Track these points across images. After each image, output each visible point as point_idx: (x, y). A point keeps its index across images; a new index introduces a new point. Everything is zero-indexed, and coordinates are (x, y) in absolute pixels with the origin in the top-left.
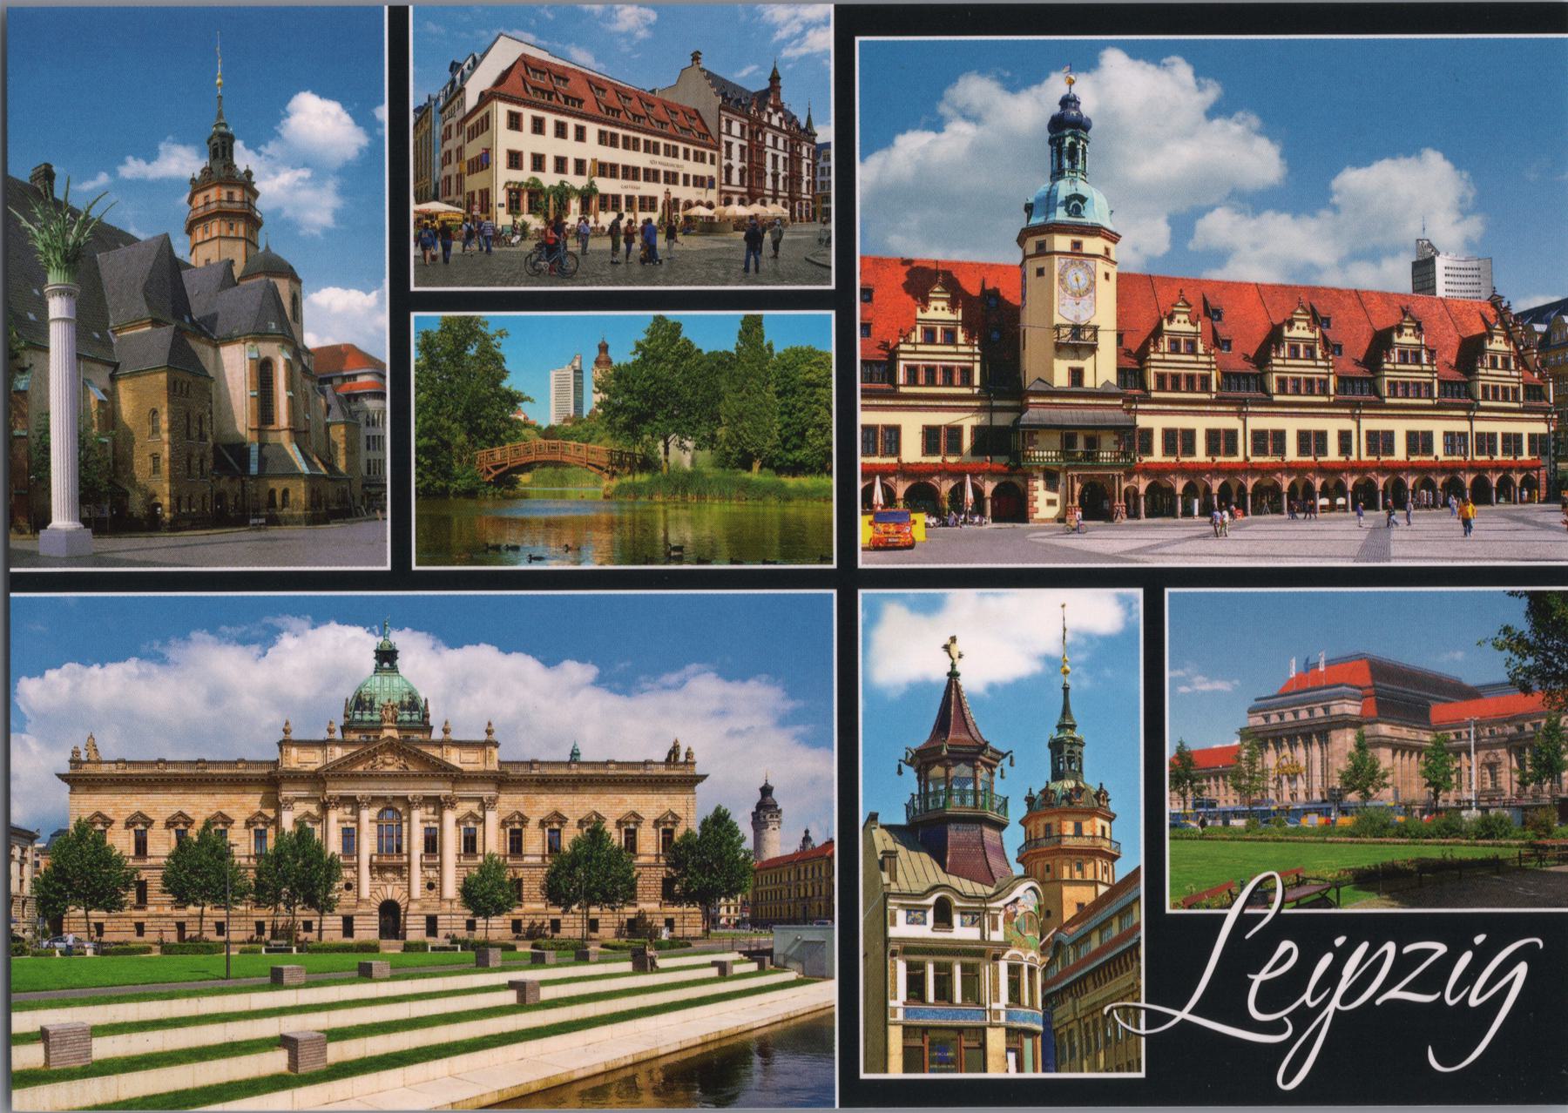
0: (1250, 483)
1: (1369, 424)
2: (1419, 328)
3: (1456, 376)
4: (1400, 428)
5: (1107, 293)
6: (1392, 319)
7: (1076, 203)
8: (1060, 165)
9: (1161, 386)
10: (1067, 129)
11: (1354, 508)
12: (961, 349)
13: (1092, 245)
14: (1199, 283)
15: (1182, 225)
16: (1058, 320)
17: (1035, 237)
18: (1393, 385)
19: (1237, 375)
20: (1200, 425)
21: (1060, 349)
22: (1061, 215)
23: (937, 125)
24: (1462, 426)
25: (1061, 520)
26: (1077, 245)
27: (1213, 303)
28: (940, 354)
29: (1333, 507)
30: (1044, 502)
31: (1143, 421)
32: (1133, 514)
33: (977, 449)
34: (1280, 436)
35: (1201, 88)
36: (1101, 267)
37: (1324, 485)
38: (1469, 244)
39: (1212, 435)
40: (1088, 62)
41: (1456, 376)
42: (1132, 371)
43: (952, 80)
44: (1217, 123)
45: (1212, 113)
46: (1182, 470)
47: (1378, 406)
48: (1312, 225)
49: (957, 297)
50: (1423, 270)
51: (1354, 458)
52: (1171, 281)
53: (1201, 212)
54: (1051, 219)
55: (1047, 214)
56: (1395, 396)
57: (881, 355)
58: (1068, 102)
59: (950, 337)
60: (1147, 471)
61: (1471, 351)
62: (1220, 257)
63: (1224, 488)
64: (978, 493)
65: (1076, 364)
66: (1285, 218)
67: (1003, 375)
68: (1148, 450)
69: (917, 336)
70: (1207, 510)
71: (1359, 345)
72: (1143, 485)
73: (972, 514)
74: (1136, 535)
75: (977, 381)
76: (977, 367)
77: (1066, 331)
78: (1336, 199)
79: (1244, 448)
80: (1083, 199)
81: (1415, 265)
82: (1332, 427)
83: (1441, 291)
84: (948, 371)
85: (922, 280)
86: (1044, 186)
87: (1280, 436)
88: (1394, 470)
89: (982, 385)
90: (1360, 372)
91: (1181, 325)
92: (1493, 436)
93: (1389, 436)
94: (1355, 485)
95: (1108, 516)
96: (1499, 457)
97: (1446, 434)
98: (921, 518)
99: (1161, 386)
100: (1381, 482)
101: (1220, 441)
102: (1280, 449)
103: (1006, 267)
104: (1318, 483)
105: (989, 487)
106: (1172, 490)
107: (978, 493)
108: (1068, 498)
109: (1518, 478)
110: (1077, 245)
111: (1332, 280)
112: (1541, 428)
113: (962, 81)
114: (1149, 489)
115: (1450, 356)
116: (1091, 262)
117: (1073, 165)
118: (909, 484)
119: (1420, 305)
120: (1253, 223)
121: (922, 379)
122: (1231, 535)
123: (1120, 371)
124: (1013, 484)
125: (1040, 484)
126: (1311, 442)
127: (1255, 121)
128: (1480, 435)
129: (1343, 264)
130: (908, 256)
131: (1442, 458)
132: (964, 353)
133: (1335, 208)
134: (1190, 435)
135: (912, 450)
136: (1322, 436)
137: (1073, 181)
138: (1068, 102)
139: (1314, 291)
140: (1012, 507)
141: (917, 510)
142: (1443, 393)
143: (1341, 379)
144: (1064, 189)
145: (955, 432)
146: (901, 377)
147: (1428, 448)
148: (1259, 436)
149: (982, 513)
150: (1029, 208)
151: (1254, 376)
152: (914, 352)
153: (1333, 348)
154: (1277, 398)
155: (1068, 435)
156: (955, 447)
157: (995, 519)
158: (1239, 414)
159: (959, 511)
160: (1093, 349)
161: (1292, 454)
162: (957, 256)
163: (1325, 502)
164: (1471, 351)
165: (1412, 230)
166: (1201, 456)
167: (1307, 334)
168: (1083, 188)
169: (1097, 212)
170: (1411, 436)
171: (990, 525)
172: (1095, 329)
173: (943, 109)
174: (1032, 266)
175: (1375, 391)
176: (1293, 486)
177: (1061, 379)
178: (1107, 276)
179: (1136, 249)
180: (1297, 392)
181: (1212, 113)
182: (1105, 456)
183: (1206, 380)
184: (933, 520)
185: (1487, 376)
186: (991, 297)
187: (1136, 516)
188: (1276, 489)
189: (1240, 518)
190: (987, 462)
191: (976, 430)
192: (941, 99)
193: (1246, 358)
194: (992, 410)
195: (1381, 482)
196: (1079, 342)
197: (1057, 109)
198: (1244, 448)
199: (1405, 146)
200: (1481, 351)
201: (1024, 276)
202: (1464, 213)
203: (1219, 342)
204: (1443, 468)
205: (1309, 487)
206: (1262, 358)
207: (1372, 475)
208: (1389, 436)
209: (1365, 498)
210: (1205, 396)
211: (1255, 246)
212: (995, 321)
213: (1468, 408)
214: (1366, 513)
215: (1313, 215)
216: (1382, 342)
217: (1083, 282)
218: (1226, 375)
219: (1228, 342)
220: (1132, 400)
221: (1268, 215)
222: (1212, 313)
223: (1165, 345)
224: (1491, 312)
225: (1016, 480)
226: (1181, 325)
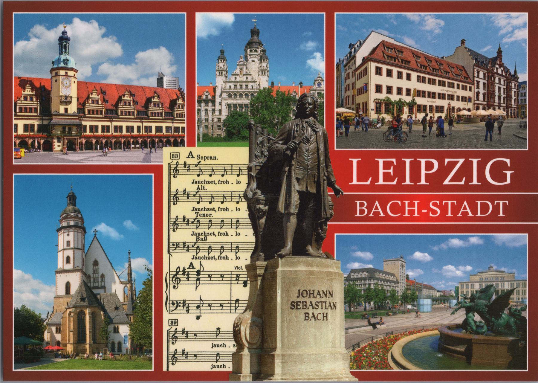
0: (113, 141)
2: (159, 97)
3: (169, 111)
4: (154, 125)
5: (74, 87)
7: (66, 61)
8: (62, 50)
10: (64, 41)
11: (141, 148)
12: (35, 102)
13: (70, 73)
14: (100, 84)
15: (95, 68)
16: (61, 94)
17: (55, 71)
18: (152, 113)
19: (110, 110)
20: (100, 124)
21: (62, 103)
22: (62, 65)
23: (28, 39)
24: (170, 125)
25: (62, 151)
26: (66, 73)
27: (103, 90)
28: (28, 104)
29: (135, 148)
30: (57, 146)
31: (84, 123)
32: (81, 149)
33: (39, 131)
34: (121, 127)
35: (100, 29)
36: (73, 79)
37: (133, 141)
38: (172, 73)
39: (103, 127)
41: (169, 111)
42: (81, 109)
43: (32, 26)
44: (105, 39)
45: (104, 36)
46: (95, 137)
48: (130, 68)
49: (33, 88)
50: (160, 81)
51: (141, 134)
52: (91, 83)
53: (100, 64)
54: (59, 66)
55: (58, 64)
56: (152, 116)
58: (64, 33)
59: (31, 99)
60: (85, 137)
61: (173, 104)
62: (105, 76)
63: (106, 142)
64: (39, 143)
65: (66, 107)
66: (123, 66)
67: (46, 110)
68: (85, 131)
69: (22, 99)
70: (101, 148)
71: (142, 102)
72: (84, 141)
73: (37, 149)
74: (81, 155)
75: (39, 111)
76: (39, 107)
77: (64, 97)
78: (136, 61)
79: (112, 130)
80: (68, 60)
81: (158, 79)
82: (135, 125)
83: (165, 87)
84: (31, 109)
85: (23, 83)
86: (57, 56)
87: (121, 127)
88: (152, 137)
89: (40, 113)
90: (143, 109)
91: (94, 96)
92: (179, 128)
93: (151, 127)
94: (141, 141)
95: (74, 150)
96: (181, 133)
97: (166, 127)
98: (23, 150)
99: (89, 113)
100: (148, 140)
101: (105, 129)
102: (121, 131)
103: (47, 79)
104: (131, 141)
105: (42, 141)
106: (92, 143)
107: (39, 143)
108: (64, 145)
110: (66, 73)
111: (135, 83)
113: (35, 26)
114: (86, 142)
115: (167, 105)
116: (70, 78)
117: (66, 50)
118: (19, 141)
119: (159, 90)
120: (115, 67)
121: (23, 111)
122: (108, 155)
123: (78, 109)
124: (49, 141)
125: (56, 141)
126: (130, 129)
127: (115, 38)
128: (175, 128)
129: (138, 79)
130: (20, 76)
131: (165, 134)
133: (136, 63)
134: (97, 127)
136: (132, 127)
137: (65, 55)
138: (64, 33)
139: (130, 86)
140: (48, 147)
141: (22, 148)
142: (165, 115)
143: (138, 111)
144: (63, 57)
145: (32, 126)
147: (161, 131)
148: (116, 127)
149: (40, 149)
150: (53, 63)
151: (115, 110)
153: (136, 103)
154: (120, 117)
155: (64, 127)
156: (32, 130)
158: (110, 121)
159: (34, 148)
160: (70, 103)
161: (124, 132)
162: (33, 76)
163: (133, 146)
164: (173, 104)
165: (157, 70)
167: (129, 99)
168: (68, 57)
170: (157, 128)
171: (42, 152)
172: (71, 97)
174: (54, 79)
175: (147, 115)
176: (124, 141)
177: (62, 111)
178: (74, 82)
179: (82, 74)
180: (126, 115)
181: (104, 36)
182: (74, 133)
183: (101, 111)
184: (26, 151)
186: (43, 88)
187: (82, 150)
188: (120, 142)
189: (111, 151)
190: (41, 134)
191: (38, 125)
192: (29, 32)
193: (112, 105)
194: (43, 120)
195: (148, 140)
196: (67, 101)
197: (61, 35)
198: (112, 130)
200: (176, 104)
201: (52, 82)
203: (105, 101)
204: (165, 137)
205: (129, 142)
206: (117, 105)
207: (146, 138)
208: (151, 127)
209: (144, 145)
210: (101, 116)
211: (115, 74)
212: (44, 94)
213: (172, 120)
214: (145, 149)
215: (130, 65)
216: (149, 101)
217: (68, 84)
218: (107, 110)
219: (108, 101)
220: (81, 117)
221: (118, 65)
222: (103, 92)
223: (90, 102)
224: (178, 93)
225: (49, 139)
226: (94, 96)
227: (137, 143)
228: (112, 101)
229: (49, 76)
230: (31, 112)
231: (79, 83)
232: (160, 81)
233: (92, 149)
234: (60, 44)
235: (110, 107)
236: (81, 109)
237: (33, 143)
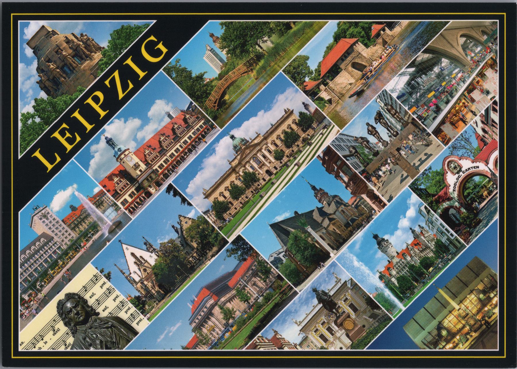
0: (175, 163)
1: (182, 141)
2: (176, 124)
3: (186, 125)
4: (186, 138)
6: (172, 126)
7: (119, 150)
9: (152, 162)
10: (110, 142)
13: (126, 153)
15: (135, 139)
17: (118, 158)
20: (162, 162)
22: (119, 153)
23: (93, 157)
24: (193, 131)
28: (121, 185)
29: (187, 156)
30: (152, 190)
31: (154, 168)
33: (137, 192)
34: (172, 153)
35: (121, 120)
36: (130, 154)
38: (172, 107)
39: (164, 161)
40: (104, 131)
41: (186, 125)
43: (89, 150)
44: (127, 123)
45: (125, 122)
46: (165, 170)
47: (181, 138)
48: (151, 124)
50: (169, 116)
53: (136, 136)
57: (114, 192)
58: (106, 138)
59: (121, 181)
60: (161, 174)
61: (185, 120)
62: (144, 139)
64: (143, 197)
66: (147, 126)
67: (132, 180)
68: (158, 171)
69: (116, 185)
70: (173, 171)
71: (170, 133)
72: (162, 176)
81: (168, 116)
82: (178, 146)
83: (174, 117)
84: (124, 186)
86: (114, 151)
87: (172, 153)
88: (190, 144)
90: (174, 136)
91: (147, 152)
93: (186, 140)
95: (161, 184)
99: (152, 162)
100: (190, 147)
102: (174, 155)
104: (183, 155)
105: (143, 195)
106: (166, 173)
107: (143, 197)
108: (154, 187)
109: (206, 130)
111: (160, 128)
112: (203, 121)
115: (183, 123)
119: (173, 121)
126: (177, 150)
127: (131, 118)
128: (196, 129)
129: (159, 125)
132: (124, 181)
133: (152, 119)
134: (161, 164)
135: (130, 200)
136: (177, 149)
139: (159, 132)
140: (149, 195)
143: (173, 139)
144: (116, 149)
145: (133, 192)
146: (120, 192)
147: (192, 137)
148: (170, 156)
149: (145, 199)
150: (114, 156)
152: (118, 188)
155: (147, 179)
156: (135, 194)
157: (148, 198)
160: (139, 165)
161: (176, 154)
162: (111, 171)
165: (163, 113)
166: (165, 165)
168: (119, 147)
169: (123, 149)
170: (188, 138)
171: (148, 200)
173: (92, 154)
175: (178, 137)
177: (139, 173)
181: (125, 122)
183: (157, 156)
185: (190, 121)
188: (178, 160)
191: (135, 189)
195: (190, 147)
196: (136, 166)
199: (152, 103)
202: (168, 104)
203: (154, 149)
204: (196, 138)
205: (182, 156)
206: (161, 146)
208: (186, 140)
209: (190, 151)
211: (147, 133)
212: (124, 174)
216: (173, 130)
218: (159, 152)
220: (150, 167)
222: (150, 146)
223: (148, 156)
224: (183, 113)
226: (147, 152)
227: (186, 153)
228: (158, 146)
229: (118, 164)
230: (126, 187)
231: (134, 153)
232: (169, 116)
233: (169, 176)
234: (110, 145)
235: (159, 150)
236: (147, 164)
237: (140, 200)
